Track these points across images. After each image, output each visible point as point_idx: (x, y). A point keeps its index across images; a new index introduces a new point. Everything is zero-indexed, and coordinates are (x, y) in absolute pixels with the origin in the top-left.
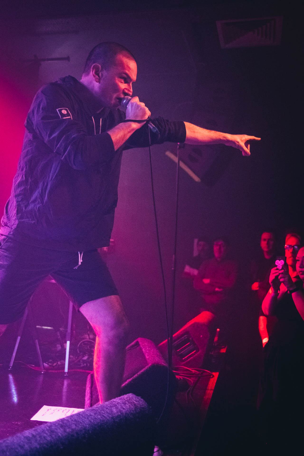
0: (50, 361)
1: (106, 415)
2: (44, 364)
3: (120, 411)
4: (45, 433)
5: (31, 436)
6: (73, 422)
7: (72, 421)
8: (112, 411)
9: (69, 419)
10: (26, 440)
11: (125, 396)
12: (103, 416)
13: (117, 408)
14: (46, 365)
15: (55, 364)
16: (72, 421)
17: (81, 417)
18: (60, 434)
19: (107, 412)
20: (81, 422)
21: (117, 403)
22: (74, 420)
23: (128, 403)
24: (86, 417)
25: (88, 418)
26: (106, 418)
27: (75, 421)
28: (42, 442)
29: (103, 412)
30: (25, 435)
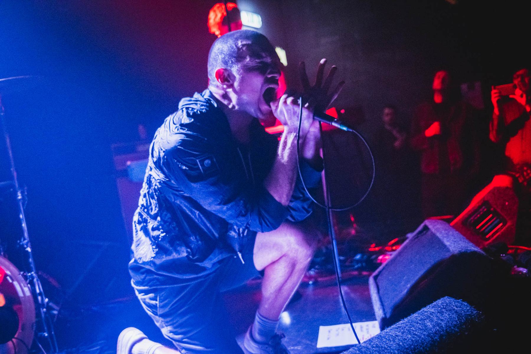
1: (418, 332)
3: (438, 324)
6: (374, 349)
7: (373, 347)
8: (426, 326)
9: (368, 345)
11: (439, 302)
12: (415, 334)
13: (432, 321)
16: (373, 347)
17: (385, 340)
19: (419, 328)
20: (386, 347)
21: (429, 312)
22: (374, 346)
23: (445, 311)
24: (391, 340)
25: (394, 341)
26: (420, 337)
27: (377, 346)
29: (414, 330)
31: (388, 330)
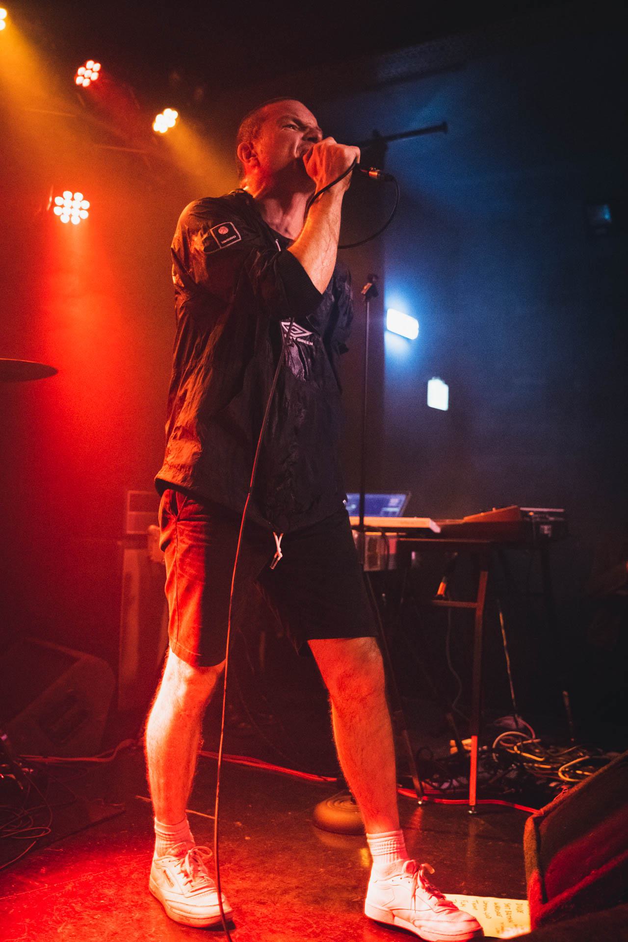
2: (423, 783)
15: (446, 785)
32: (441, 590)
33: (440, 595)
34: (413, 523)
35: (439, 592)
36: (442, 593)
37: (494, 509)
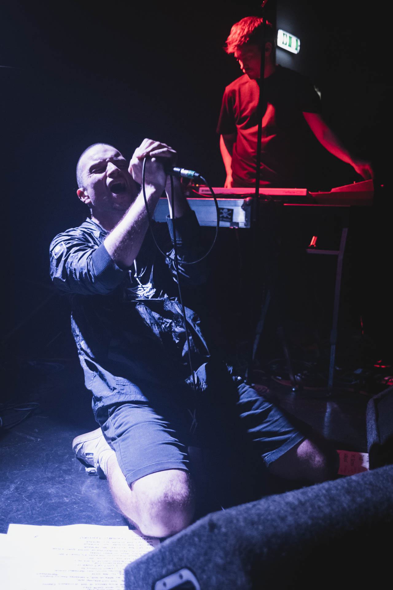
0: (305, 372)
2: (296, 376)
4: (320, 500)
5: (296, 503)
7: (366, 484)
10: (289, 510)
14: (298, 377)
17: (381, 479)
18: (345, 505)
20: (382, 487)
22: (368, 482)
27: (371, 484)
28: (315, 514)
30: (287, 500)
31: (387, 468)
32: (313, 241)
33: (313, 245)
34: (294, 192)
35: (312, 243)
36: (314, 244)
37: (354, 182)
